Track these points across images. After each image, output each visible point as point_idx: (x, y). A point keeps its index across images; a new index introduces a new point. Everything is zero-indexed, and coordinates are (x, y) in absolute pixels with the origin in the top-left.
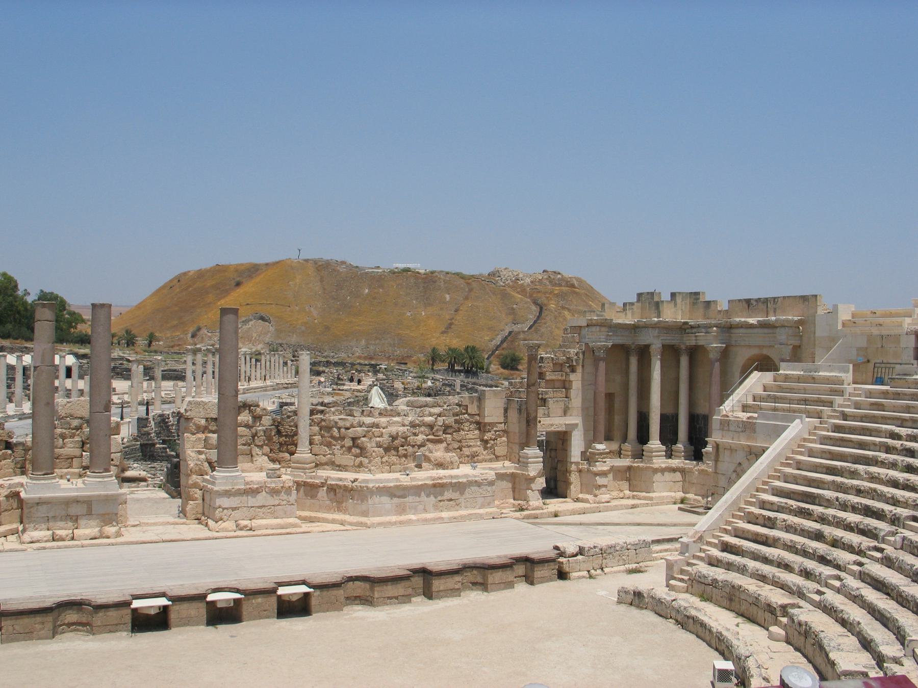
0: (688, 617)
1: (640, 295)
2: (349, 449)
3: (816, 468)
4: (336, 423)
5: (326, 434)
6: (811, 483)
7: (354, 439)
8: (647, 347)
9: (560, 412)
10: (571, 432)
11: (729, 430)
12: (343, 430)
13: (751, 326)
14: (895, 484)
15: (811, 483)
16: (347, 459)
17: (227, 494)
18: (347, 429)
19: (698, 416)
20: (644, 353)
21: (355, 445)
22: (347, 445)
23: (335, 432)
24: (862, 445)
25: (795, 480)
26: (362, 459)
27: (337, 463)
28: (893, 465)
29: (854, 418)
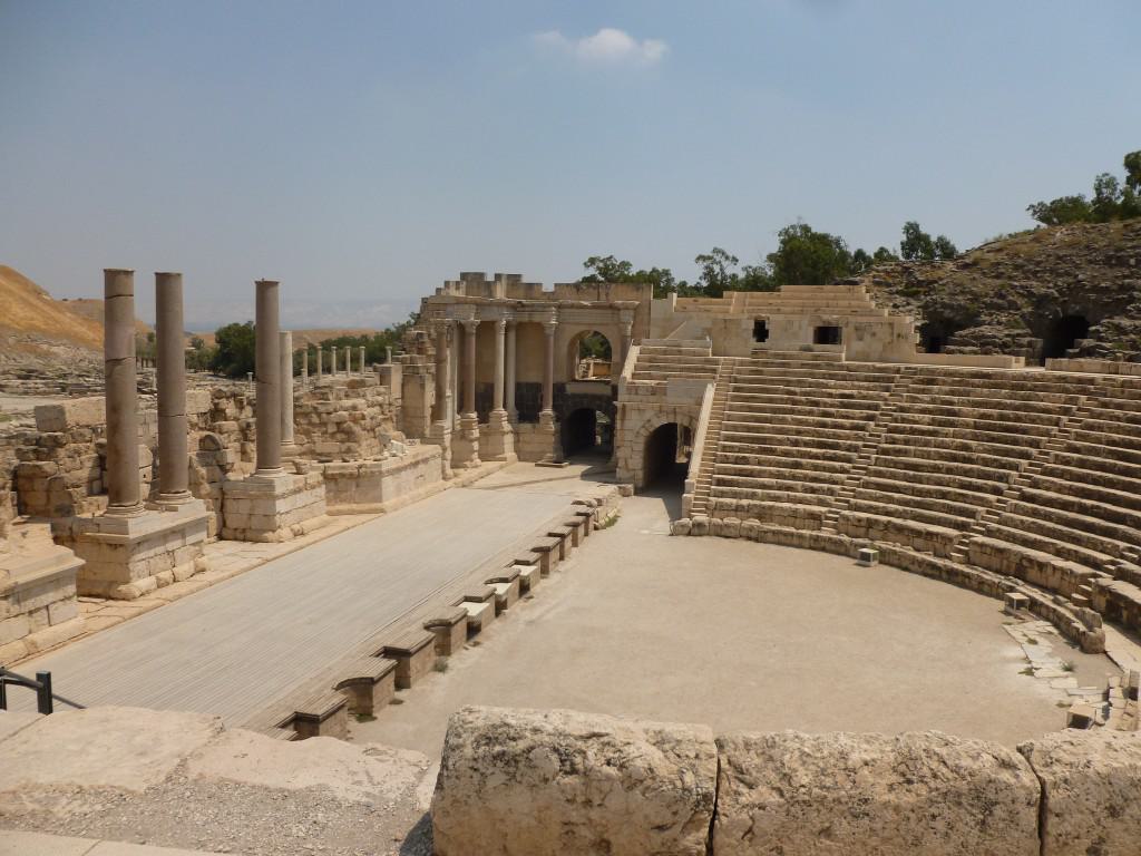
0: (765, 532)
1: (464, 276)
2: (333, 434)
3: (745, 419)
4: (315, 408)
5: (302, 421)
6: (749, 429)
7: (338, 424)
8: (493, 323)
11: (637, 394)
12: (324, 415)
14: (824, 425)
15: (749, 429)
16: (331, 446)
17: (283, 496)
18: (329, 413)
20: (487, 329)
21: (340, 430)
22: (330, 431)
23: (315, 419)
24: (771, 400)
25: (735, 428)
26: (348, 444)
27: (318, 451)
28: (810, 413)
29: (745, 381)
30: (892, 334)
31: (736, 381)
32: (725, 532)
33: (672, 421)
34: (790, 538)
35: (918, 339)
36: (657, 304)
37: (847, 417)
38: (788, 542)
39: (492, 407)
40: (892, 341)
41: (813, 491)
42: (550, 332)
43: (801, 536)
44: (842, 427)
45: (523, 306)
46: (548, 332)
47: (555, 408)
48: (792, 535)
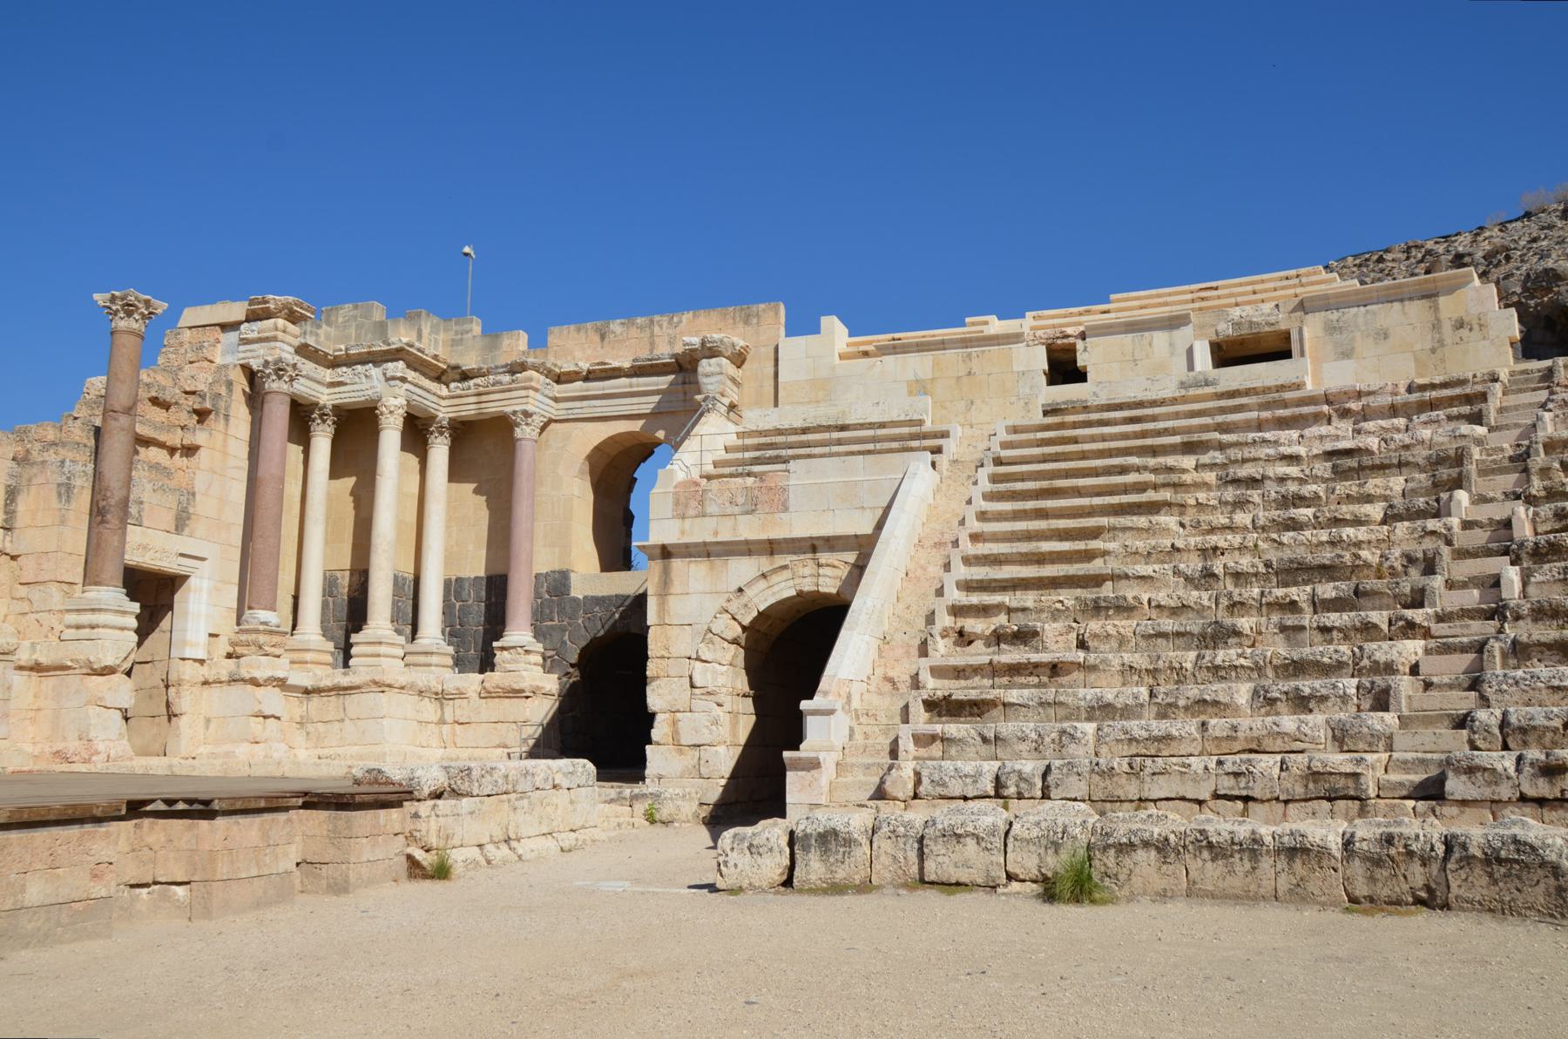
9: (168, 519)
13: (615, 373)
14: (1294, 525)
28: (1240, 504)
30: (1436, 326)
31: (998, 462)
32: (941, 863)
33: (808, 586)
34: (1242, 865)
35: (1510, 325)
36: (795, 349)
37: (1368, 499)
38: (1235, 883)
40: (1441, 342)
41: (1301, 703)
43: (1296, 851)
44: (1357, 522)
45: (465, 376)
48: (1253, 849)
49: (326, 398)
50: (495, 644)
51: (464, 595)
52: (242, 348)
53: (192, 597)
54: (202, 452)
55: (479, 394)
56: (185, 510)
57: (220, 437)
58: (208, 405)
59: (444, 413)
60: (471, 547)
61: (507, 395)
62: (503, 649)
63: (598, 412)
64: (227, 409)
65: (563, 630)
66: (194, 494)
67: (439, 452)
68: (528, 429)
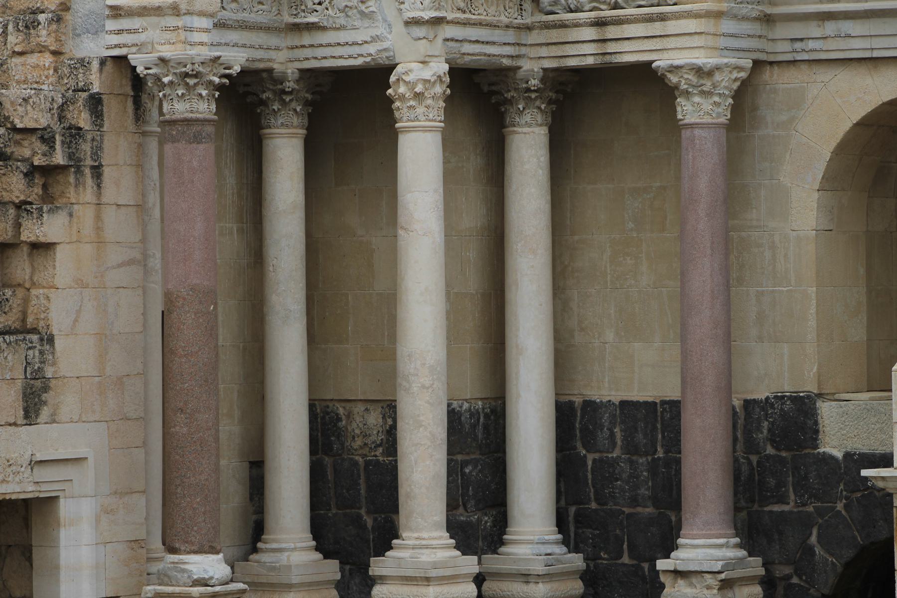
10: (52, 501)
19: (589, 405)
39: (386, 535)
42: (699, 111)
46: (690, 110)
47: (752, 531)
49: (285, 59)
50: (662, 564)
51: (602, 436)
52: (111, 25)
53: (65, 535)
54: (61, 253)
55: (600, 23)
56: (38, 374)
57: (86, 215)
58: (59, 158)
59: (533, 66)
60: (610, 336)
61: (656, 28)
62: (678, 574)
63: (858, 47)
64: (96, 153)
65: (805, 523)
66: (51, 340)
67: (529, 146)
68: (707, 105)
